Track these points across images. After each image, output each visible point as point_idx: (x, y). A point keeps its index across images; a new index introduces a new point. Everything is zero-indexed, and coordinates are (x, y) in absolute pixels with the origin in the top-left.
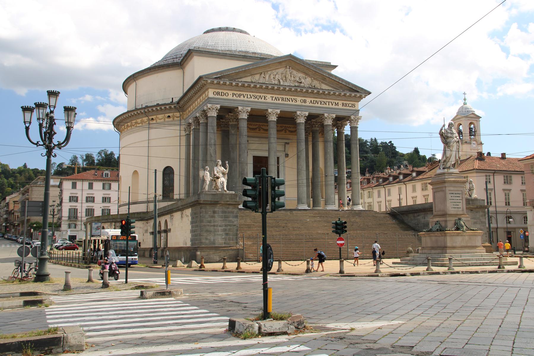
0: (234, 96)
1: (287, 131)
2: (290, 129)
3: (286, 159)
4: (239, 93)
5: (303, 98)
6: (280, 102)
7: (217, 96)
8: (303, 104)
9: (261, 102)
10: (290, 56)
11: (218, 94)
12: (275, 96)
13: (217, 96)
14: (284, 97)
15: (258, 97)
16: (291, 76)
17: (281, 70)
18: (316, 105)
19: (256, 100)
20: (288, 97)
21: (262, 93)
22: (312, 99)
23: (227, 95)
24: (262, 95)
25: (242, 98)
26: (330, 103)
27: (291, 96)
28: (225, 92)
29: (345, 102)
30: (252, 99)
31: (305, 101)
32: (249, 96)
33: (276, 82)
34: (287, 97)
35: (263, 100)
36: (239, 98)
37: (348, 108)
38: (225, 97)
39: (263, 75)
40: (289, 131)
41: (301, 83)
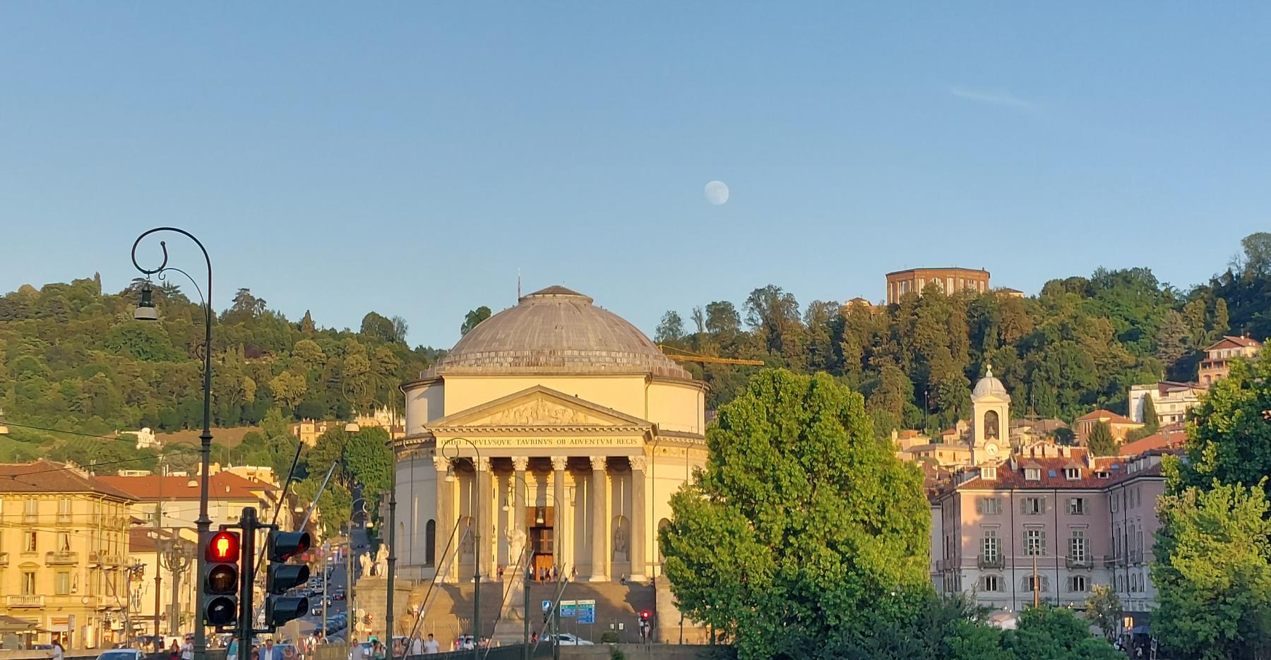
6: (529, 445)
17: (533, 403)
18: (579, 445)
30: (492, 446)
31: (563, 442)
33: (524, 421)
35: (506, 446)
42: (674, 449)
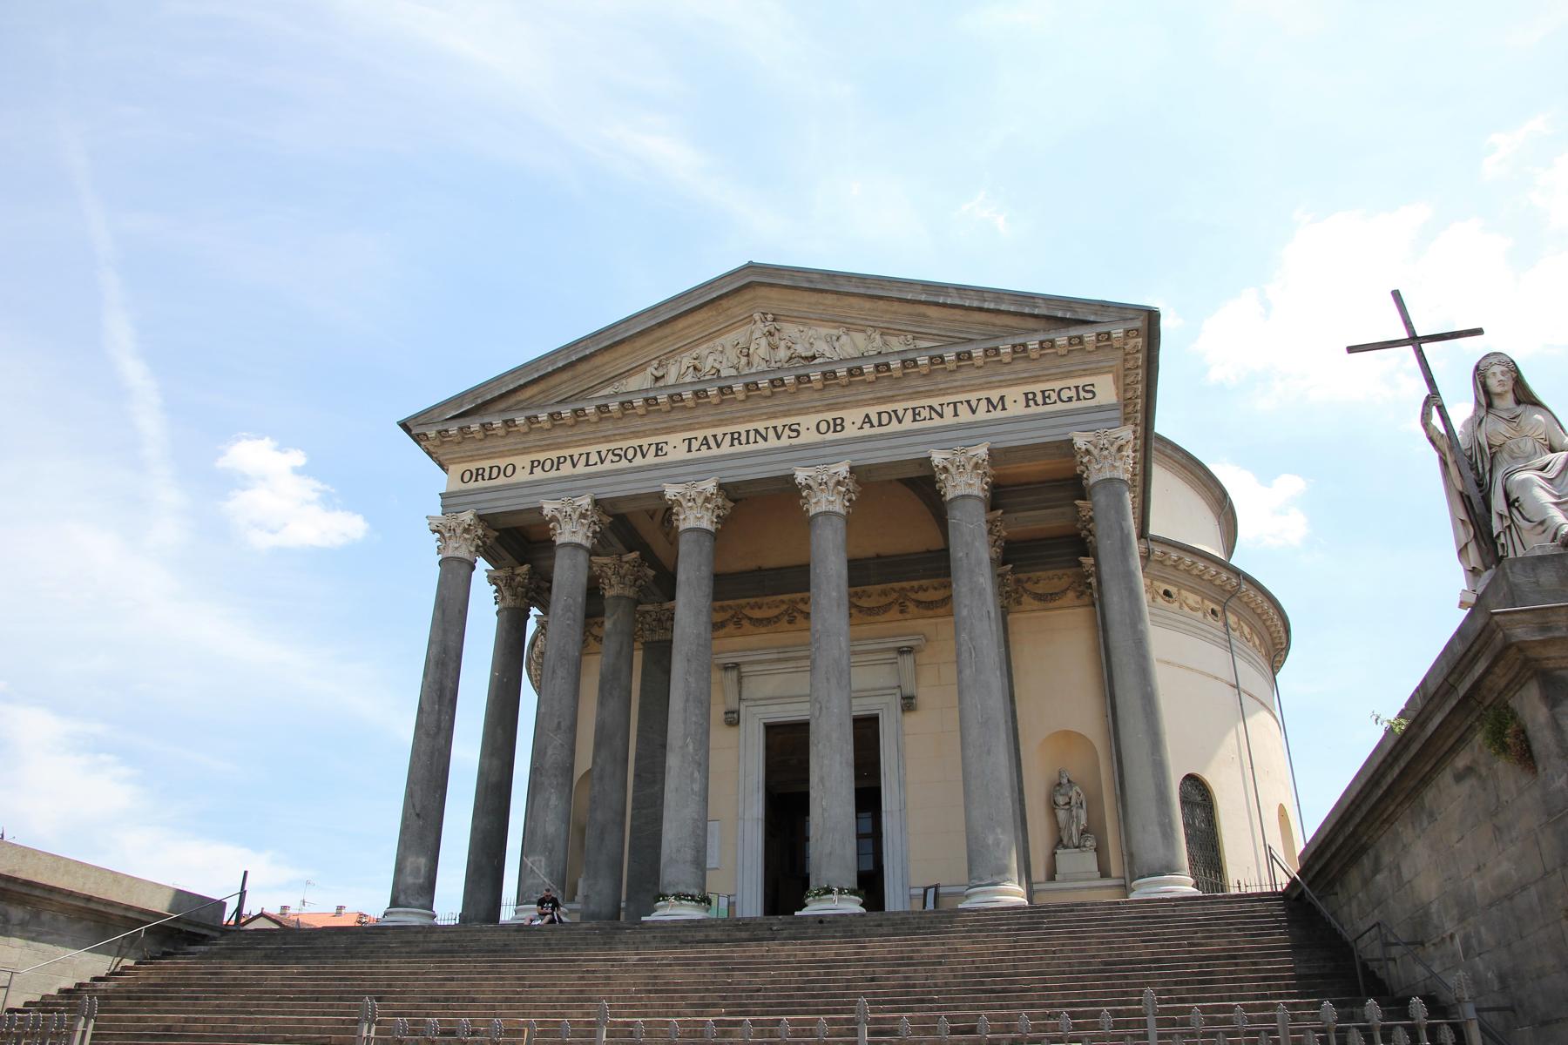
0: (538, 470)
1: (911, 607)
2: (922, 596)
3: (911, 718)
4: (554, 455)
5: (829, 416)
6: (726, 448)
7: (472, 485)
8: (831, 436)
9: (640, 469)
10: (751, 267)
11: (478, 474)
12: (700, 434)
13: (472, 485)
14: (742, 428)
15: (630, 454)
16: (774, 347)
18: (895, 426)
19: (624, 463)
20: (760, 426)
21: (645, 434)
22: (873, 412)
23: (509, 472)
24: (645, 442)
25: (566, 469)
26: (963, 410)
27: (774, 416)
28: (502, 463)
29: (1037, 388)
30: (607, 466)
31: (838, 425)
32: (594, 458)
34: (751, 426)
35: (651, 459)
36: (553, 474)
37: (1060, 406)
38: (502, 480)
39: (651, 370)
40: (919, 603)
41: (814, 357)
42: (1192, 599)
